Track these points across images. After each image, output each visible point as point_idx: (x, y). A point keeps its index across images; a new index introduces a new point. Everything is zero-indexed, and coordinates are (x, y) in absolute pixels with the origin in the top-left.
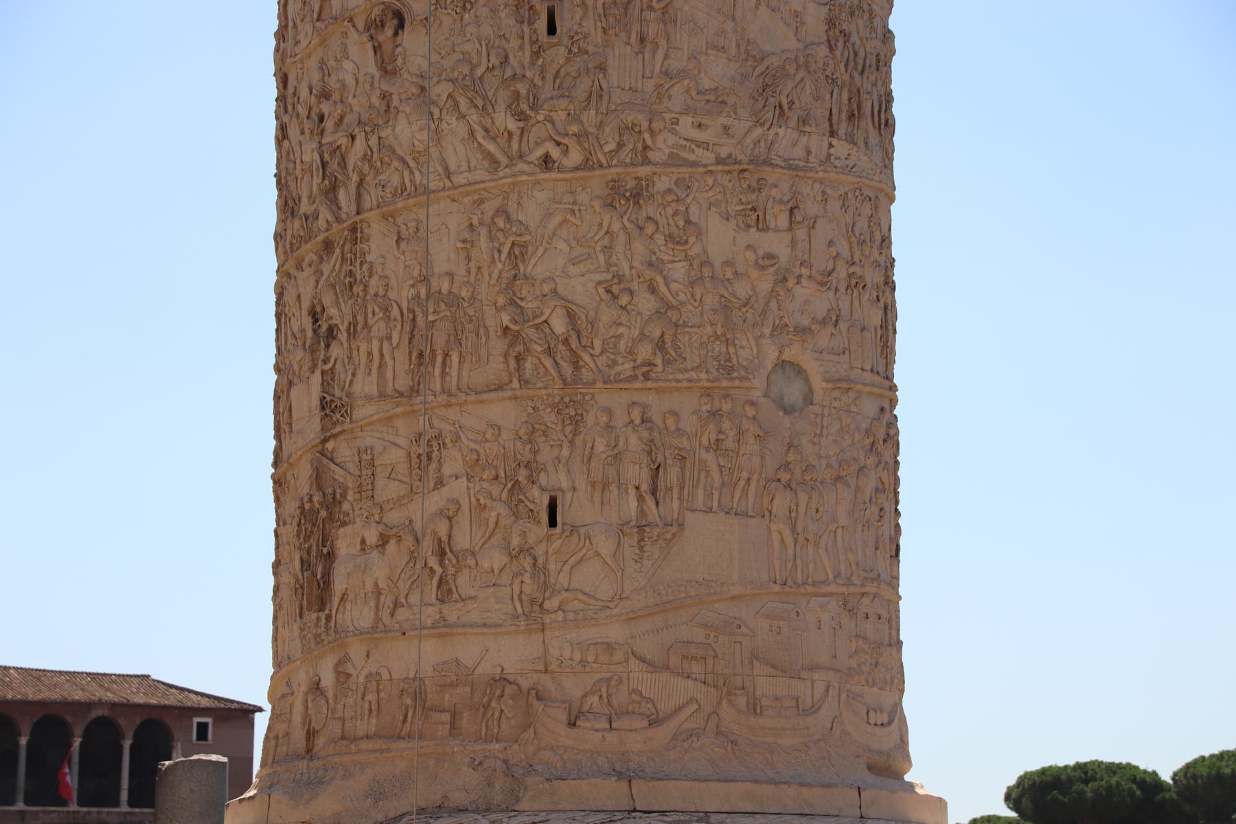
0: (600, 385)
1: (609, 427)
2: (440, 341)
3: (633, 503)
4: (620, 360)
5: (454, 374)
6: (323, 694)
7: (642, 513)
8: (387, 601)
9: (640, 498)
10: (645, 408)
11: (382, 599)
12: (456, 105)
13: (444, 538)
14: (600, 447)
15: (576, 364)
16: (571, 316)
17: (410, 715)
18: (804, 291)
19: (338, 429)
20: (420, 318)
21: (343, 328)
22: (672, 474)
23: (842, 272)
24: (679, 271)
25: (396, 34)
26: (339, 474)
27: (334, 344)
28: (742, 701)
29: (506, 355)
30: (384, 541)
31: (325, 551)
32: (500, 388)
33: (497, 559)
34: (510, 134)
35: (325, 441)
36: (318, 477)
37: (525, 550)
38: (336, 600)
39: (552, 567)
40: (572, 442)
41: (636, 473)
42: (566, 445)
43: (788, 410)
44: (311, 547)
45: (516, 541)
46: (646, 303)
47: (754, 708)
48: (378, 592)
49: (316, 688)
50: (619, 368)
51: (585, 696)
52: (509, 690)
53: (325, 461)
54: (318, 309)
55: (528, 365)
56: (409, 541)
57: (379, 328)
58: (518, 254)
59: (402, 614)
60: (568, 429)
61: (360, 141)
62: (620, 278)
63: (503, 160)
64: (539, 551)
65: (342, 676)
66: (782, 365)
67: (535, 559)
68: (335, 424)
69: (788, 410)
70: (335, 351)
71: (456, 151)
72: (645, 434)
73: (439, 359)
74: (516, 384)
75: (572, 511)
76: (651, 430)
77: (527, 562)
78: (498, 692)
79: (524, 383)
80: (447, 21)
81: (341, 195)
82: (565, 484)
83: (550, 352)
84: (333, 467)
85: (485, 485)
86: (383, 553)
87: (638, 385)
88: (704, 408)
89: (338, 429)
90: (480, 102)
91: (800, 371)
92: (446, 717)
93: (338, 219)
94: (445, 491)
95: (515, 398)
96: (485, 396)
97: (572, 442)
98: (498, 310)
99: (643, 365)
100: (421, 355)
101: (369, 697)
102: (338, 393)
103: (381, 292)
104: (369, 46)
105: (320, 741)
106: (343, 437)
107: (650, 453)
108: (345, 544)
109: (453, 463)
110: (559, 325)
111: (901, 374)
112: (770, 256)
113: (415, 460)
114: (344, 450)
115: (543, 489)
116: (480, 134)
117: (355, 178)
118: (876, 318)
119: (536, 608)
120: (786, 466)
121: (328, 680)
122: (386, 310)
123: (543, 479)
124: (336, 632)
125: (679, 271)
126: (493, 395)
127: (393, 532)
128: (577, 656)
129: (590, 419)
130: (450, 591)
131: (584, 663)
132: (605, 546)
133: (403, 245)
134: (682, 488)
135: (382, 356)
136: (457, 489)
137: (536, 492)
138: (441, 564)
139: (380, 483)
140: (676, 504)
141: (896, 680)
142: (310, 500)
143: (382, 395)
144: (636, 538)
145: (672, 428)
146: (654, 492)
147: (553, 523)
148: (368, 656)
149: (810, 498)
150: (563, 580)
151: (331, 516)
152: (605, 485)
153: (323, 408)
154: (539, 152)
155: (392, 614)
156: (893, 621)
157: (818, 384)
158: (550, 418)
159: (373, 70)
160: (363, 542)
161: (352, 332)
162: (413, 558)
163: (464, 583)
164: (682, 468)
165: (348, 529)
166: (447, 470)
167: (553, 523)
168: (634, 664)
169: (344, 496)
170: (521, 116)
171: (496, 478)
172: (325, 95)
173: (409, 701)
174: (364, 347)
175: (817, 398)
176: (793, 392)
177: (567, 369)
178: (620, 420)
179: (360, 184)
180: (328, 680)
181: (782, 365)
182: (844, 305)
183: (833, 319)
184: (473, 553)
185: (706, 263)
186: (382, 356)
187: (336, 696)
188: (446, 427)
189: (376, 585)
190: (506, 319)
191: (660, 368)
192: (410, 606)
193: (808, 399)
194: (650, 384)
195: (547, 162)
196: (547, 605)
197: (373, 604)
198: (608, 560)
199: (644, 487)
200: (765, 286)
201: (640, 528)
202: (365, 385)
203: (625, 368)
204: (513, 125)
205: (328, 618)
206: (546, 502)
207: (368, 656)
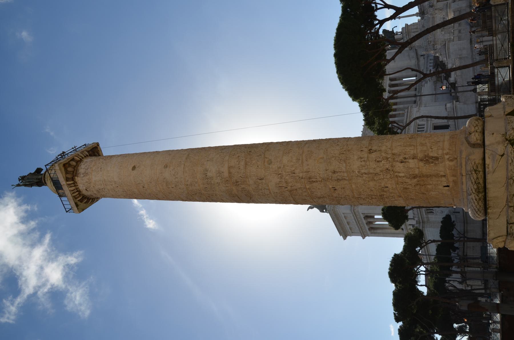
30: (432, 149)
36: (421, 160)
48: (438, 149)
65: (447, 154)
70: (407, 157)
81: (388, 157)
104: (372, 153)
108: (431, 154)
117: (387, 155)
174: (408, 152)
179: (387, 154)
205: (440, 157)
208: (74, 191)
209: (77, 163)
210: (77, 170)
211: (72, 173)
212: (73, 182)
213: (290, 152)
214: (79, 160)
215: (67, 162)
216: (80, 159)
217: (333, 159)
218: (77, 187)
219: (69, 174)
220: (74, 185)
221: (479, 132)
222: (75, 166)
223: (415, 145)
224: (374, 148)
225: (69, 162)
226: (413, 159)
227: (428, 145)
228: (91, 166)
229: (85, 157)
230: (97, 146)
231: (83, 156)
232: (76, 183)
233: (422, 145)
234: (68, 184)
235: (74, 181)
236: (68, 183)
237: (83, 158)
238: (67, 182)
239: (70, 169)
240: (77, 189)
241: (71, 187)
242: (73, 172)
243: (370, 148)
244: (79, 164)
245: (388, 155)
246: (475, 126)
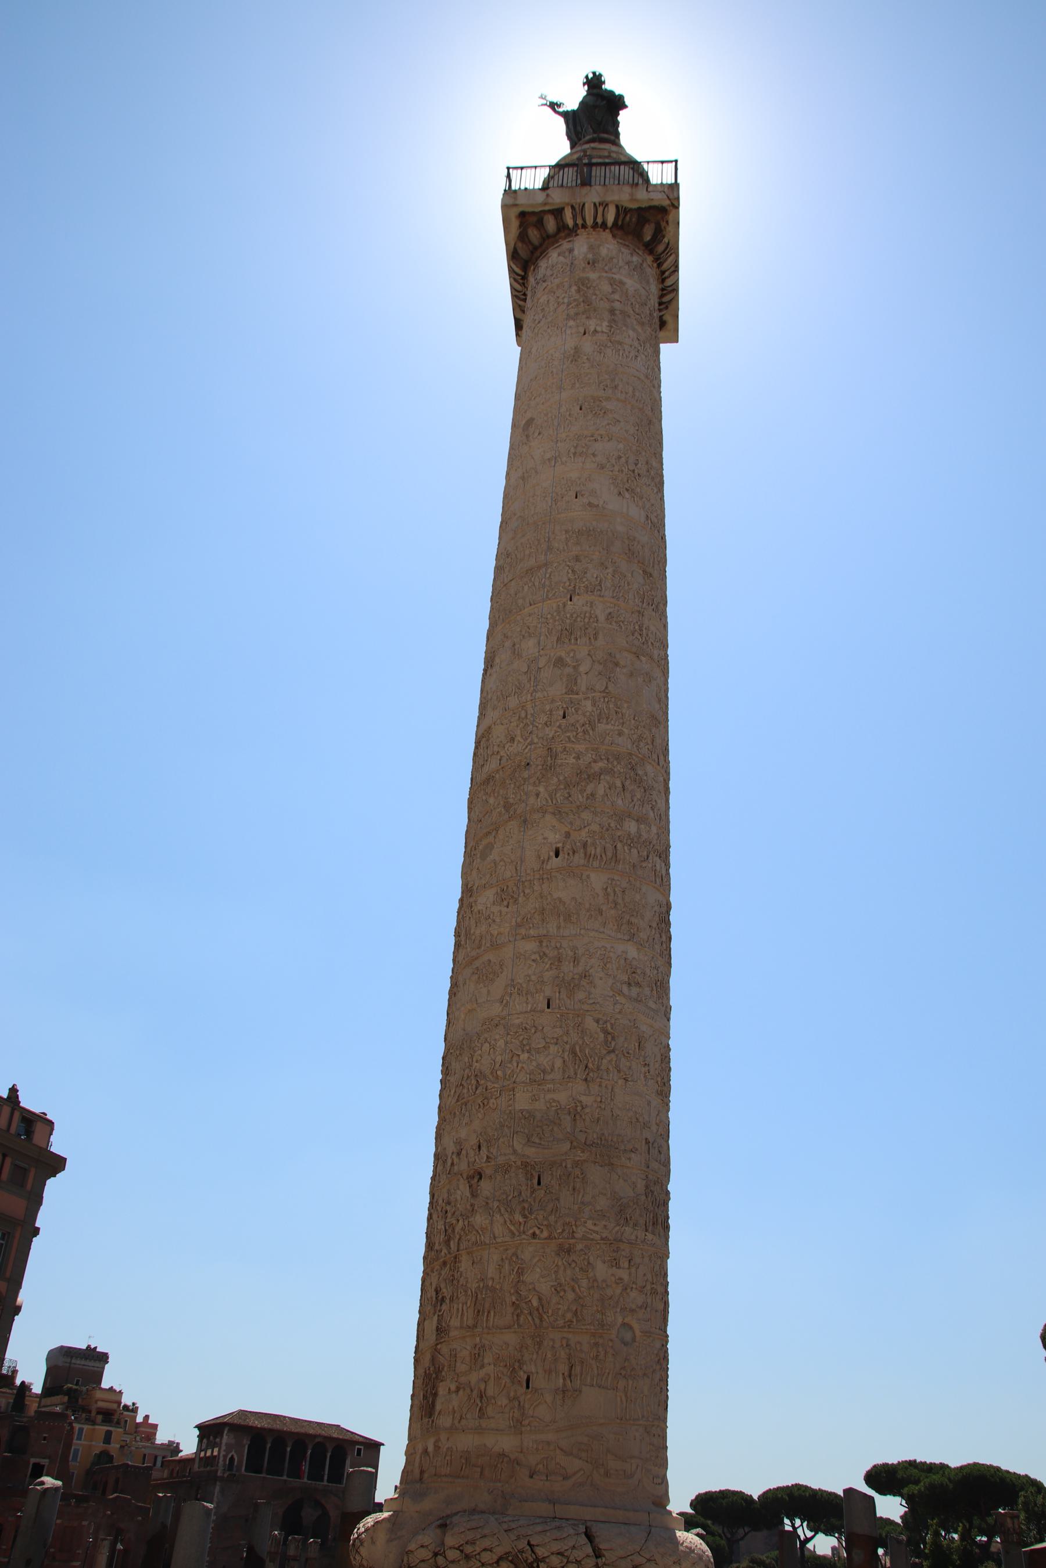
0: (550, 1329)
1: (553, 1347)
2: (487, 1305)
3: (561, 1381)
4: (559, 1319)
5: (492, 1320)
6: (428, 1455)
7: (564, 1385)
8: (457, 1415)
9: (564, 1379)
10: (568, 1340)
11: (456, 1415)
12: (500, 1210)
13: (483, 1391)
14: (549, 1355)
15: (541, 1320)
16: (540, 1299)
17: (464, 1467)
18: (634, 1294)
19: (443, 1340)
20: (479, 1296)
21: (448, 1298)
22: (577, 1369)
23: (649, 1287)
24: (584, 1283)
25: (478, 1181)
26: (442, 1359)
27: (444, 1304)
28: (602, 1471)
29: (513, 1314)
31: (433, 1392)
32: (509, 1327)
33: (503, 1401)
34: (520, 1223)
35: (437, 1344)
36: (433, 1359)
37: (516, 1398)
38: (437, 1414)
39: (527, 1406)
40: (537, 1353)
41: (563, 1368)
42: (535, 1354)
43: (625, 1344)
44: (427, 1390)
45: (512, 1394)
46: (571, 1296)
47: (607, 1474)
49: (425, 1451)
50: (559, 1322)
51: (537, 1464)
52: (506, 1459)
53: (436, 1353)
54: (439, 1289)
55: (522, 1319)
56: (468, 1391)
57: (462, 1299)
58: (520, 1272)
59: (464, 1422)
60: (536, 1347)
61: (461, 1222)
62: (560, 1285)
63: (517, 1233)
64: (522, 1399)
65: (437, 1447)
66: (624, 1324)
67: (520, 1402)
68: (442, 1338)
69: (625, 1344)
70: (444, 1307)
71: (498, 1229)
72: (567, 1351)
73: (486, 1314)
74: (516, 1326)
75: (537, 1382)
76: (570, 1349)
77: (516, 1403)
78: (501, 1460)
79: (519, 1326)
80: (499, 1178)
81: (452, 1243)
82: (533, 1370)
83: (531, 1314)
84: (440, 1356)
85: (501, 1369)
86: (457, 1394)
87: (566, 1330)
88: (592, 1342)
89: (443, 1340)
90: (509, 1210)
91: (631, 1328)
92: (479, 1470)
93: (449, 1253)
94: (484, 1370)
95: (515, 1332)
96: (504, 1331)
97: (537, 1353)
98: (511, 1294)
99: (568, 1321)
100: (479, 1311)
101: (447, 1458)
102: (444, 1324)
103: (465, 1284)
105: (426, 1475)
106: (444, 1344)
107: (569, 1359)
108: (442, 1391)
109: (488, 1358)
110: (535, 1303)
111: (670, 1331)
112: (621, 1279)
113: (473, 1357)
114: (444, 1349)
115: (525, 1372)
116: (508, 1223)
117: (458, 1237)
118: (662, 1307)
119: (519, 1424)
120: (624, 1368)
121: (431, 1449)
122: (466, 1291)
123: (525, 1368)
124: (436, 1428)
125: (584, 1283)
126: (506, 1330)
127: (462, 1386)
128: (535, 1447)
129: (545, 1343)
130: (484, 1414)
131: (537, 1449)
132: (549, 1398)
133: (475, 1265)
134: (581, 1375)
135: (463, 1310)
136: (489, 1369)
137: (522, 1373)
138: (481, 1401)
139: (458, 1364)
140: (579, 1381)
141: (664, 1464)
142: (429, 1369)
143: (461, 1327)
144: (561, 1396)
145: (578, 1349)
146: (570, 1376)
147: (528, 1387)
148: (448, 1439)
149: (633, 1382)
150: (531, 1412)
151: (437, 1377)
152: (550, 1372)
153: (437, 1331)
154: (531, 1231)
155: (459, 1422)
156: (664, 1438)
157: (638, 1333)
158: (529, 1342)
159: (468, 1194)
160: (449, 1389)
161: (451, 1300)
162: (469, 1398)
163: (490, 1411)
164: (582, 1367)
165: (444, 1383)
166: (486, 1361)
167: (528, 1387)
168: (558, 1451)
169: (443, 1369)
170: (525, 1217)
171: (506, 1366)
172: (449, 1203)
173: (464, 1461)
174: (456, 1306)
175: (637, 1340)
176: (628, 1336)
177: (537, 1321)
178: (557, 1345)
179: (459, 1239)
180: (431, 1449)
181: (624, 1324)
182: (649, 1301)
183: (645, 1306)
184: (494, 1398)
185: (595, 1280)
186: (463, 1310)
187: (433, 1456)
188: (487, 1343)
189: (454, 1408)
190: (514, 1299)
191: (575, 1323)
192: (467, 1419)
193: (634, 1339)
194: (570, 1330)
195: (534, 1235)
196: (523, 1423)
197: (451, 1417)
198: (550, 1405)
199: (566, 1374)
200: (618, 1291)
201: (563, 1391)
202: (455, 1322)
203: (561, 1322)
204: (521, 1220)
205: (433, 1421)
206: (526, 1378)
207: (448, 1439)
209: (559, 230)
212: (523, 274)
213: (505, 903)
214: (568, 225)
215: (537, 210)
217: (466, 1059)
219: (524, 246)
221: (436, 1562)
222: (548, 237)
223: (479, 1329)
224: (486, 1187)
225: (544, 212)
226: (437, 1329)
227: (474, 1378)
229: (595, 225)
230: (668, 208)
231: (590, 221)
233: (476, 1358)
235: (525, 273)
237: (584, 226)
239: (534, 234)
243: (488, 1171)
245: (457, 1240)
246: (462, 1551)
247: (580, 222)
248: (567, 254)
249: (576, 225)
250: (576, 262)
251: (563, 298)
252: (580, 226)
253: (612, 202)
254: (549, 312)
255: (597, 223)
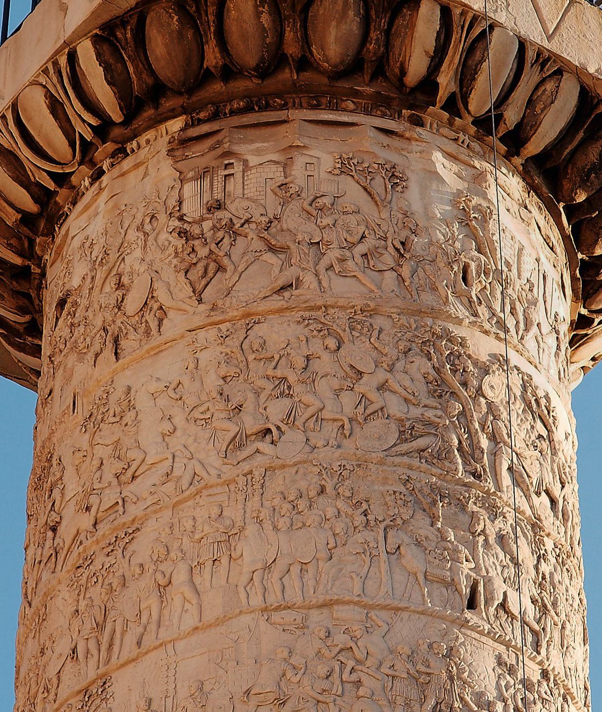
208: (25, 153)
210: (267, 107)
211: (213, 57)
212: (116, 116)
214: (403, 72)
216: (428, 85)
218: (81, 176)
219: (190, 34)
220: (88, 136)
222: (304, 63)
228: (309, 279)
232: (121, 153)
234: (72, 58)
236: (86, 52)
238: (97, 41)
240: (61, 179)
241: (55, 107)
242: (229, 72)
244: (356, 94)
247: (446, 81)
248: (378, 185)
249: (428, 85)
250: (418, 242)
251: (382, 387)
252: (442, 95)
253: (579, 73)
254: (317, 417)
255: (499, 118)
